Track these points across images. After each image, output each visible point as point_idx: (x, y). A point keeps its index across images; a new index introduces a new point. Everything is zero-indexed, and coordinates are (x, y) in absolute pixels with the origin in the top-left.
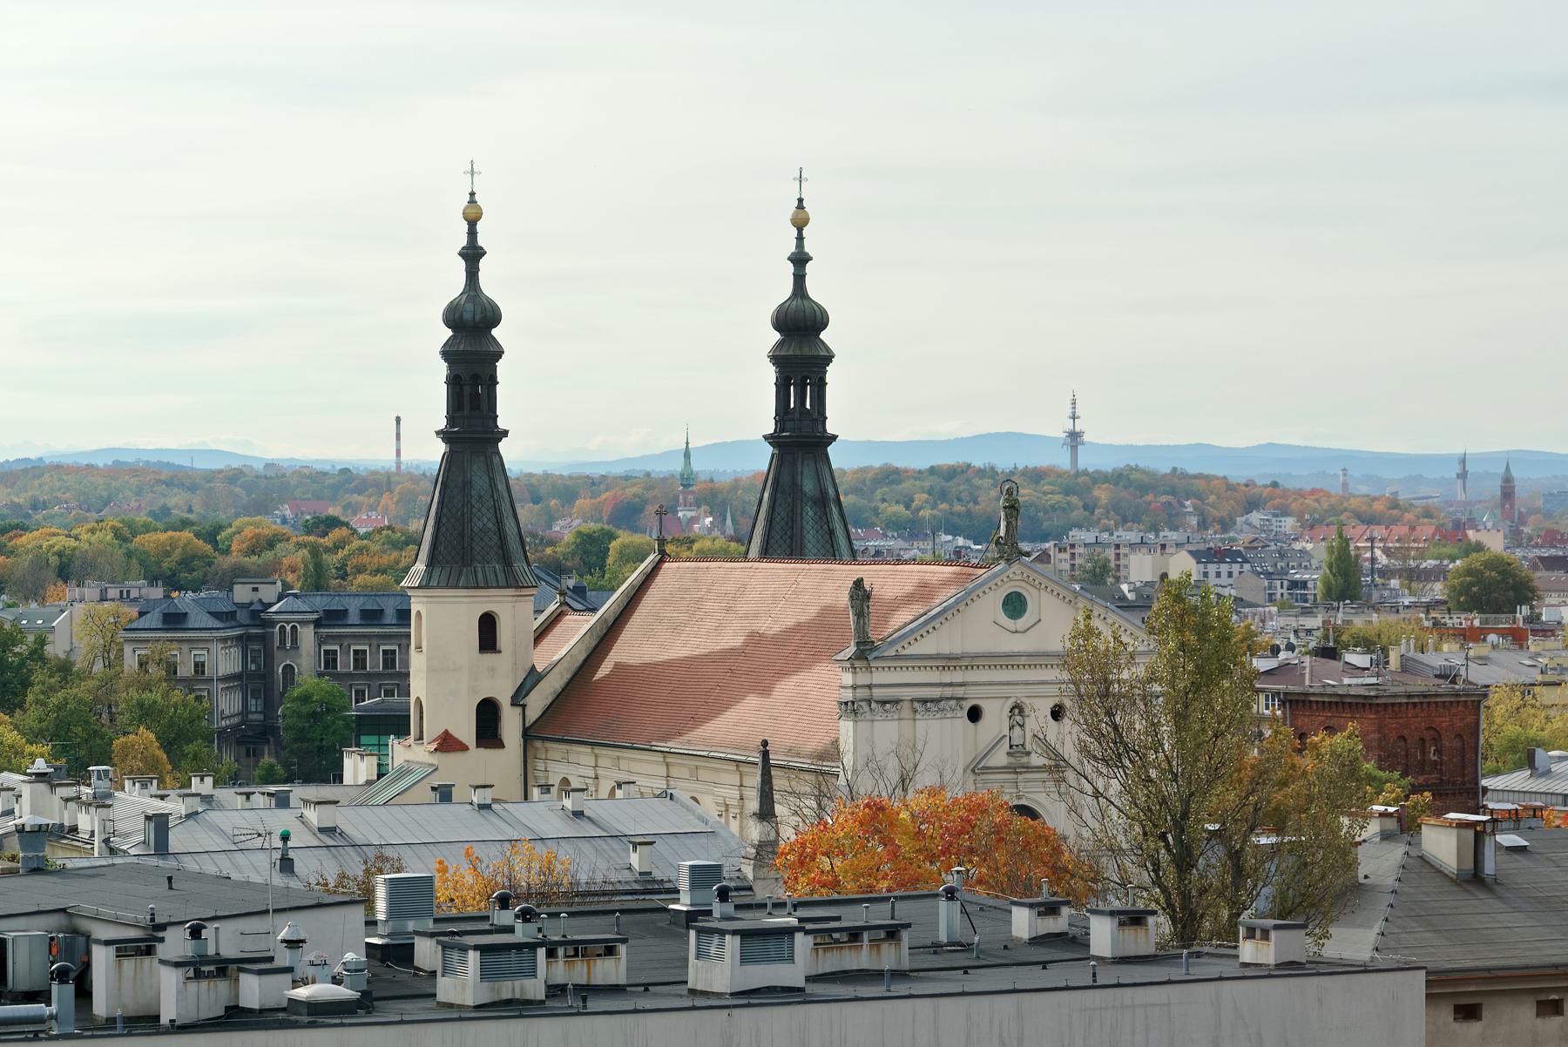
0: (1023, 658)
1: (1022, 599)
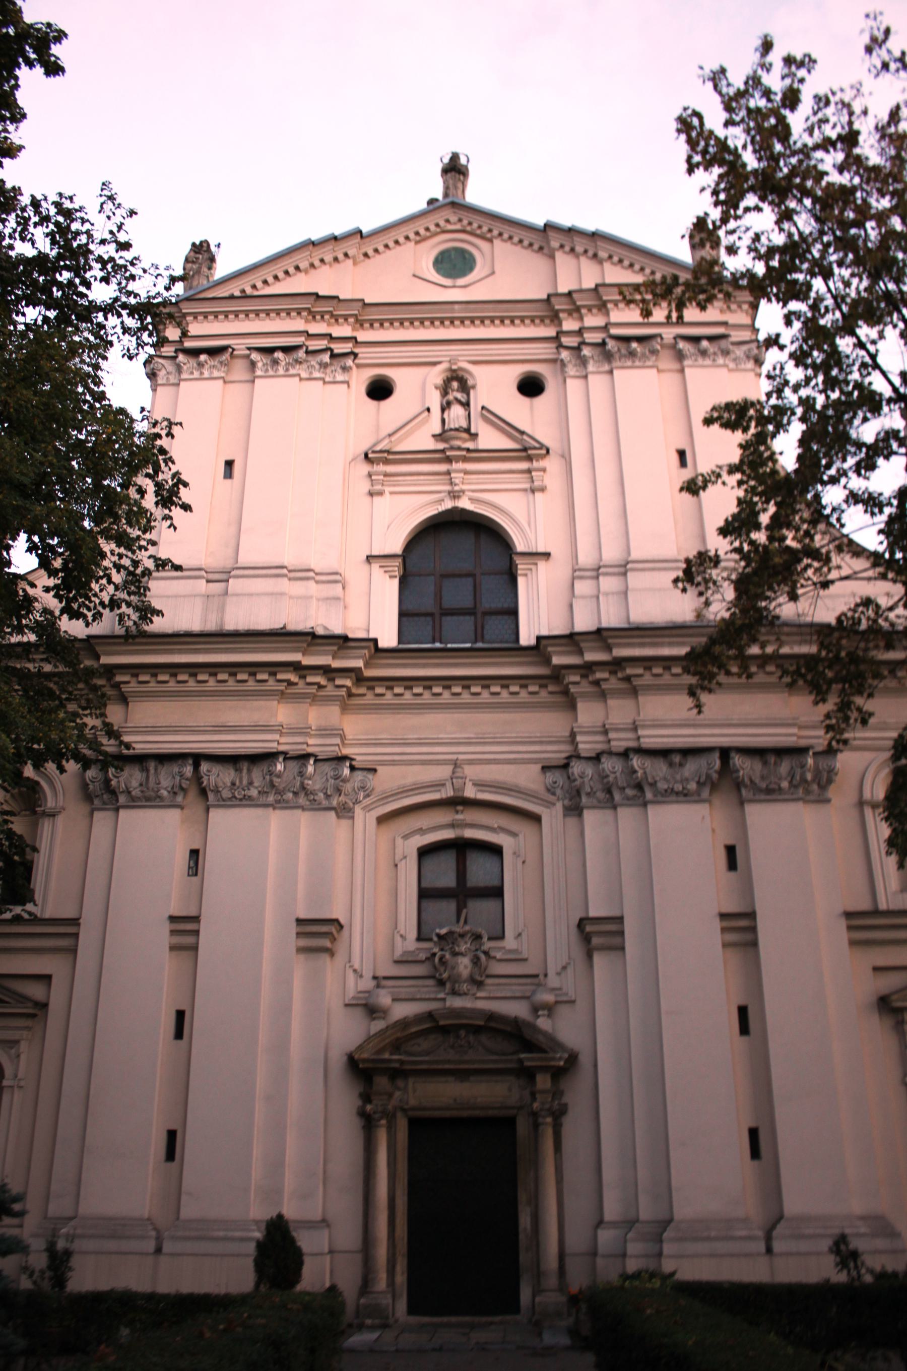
0: (456, 307)
1: (467, 256)
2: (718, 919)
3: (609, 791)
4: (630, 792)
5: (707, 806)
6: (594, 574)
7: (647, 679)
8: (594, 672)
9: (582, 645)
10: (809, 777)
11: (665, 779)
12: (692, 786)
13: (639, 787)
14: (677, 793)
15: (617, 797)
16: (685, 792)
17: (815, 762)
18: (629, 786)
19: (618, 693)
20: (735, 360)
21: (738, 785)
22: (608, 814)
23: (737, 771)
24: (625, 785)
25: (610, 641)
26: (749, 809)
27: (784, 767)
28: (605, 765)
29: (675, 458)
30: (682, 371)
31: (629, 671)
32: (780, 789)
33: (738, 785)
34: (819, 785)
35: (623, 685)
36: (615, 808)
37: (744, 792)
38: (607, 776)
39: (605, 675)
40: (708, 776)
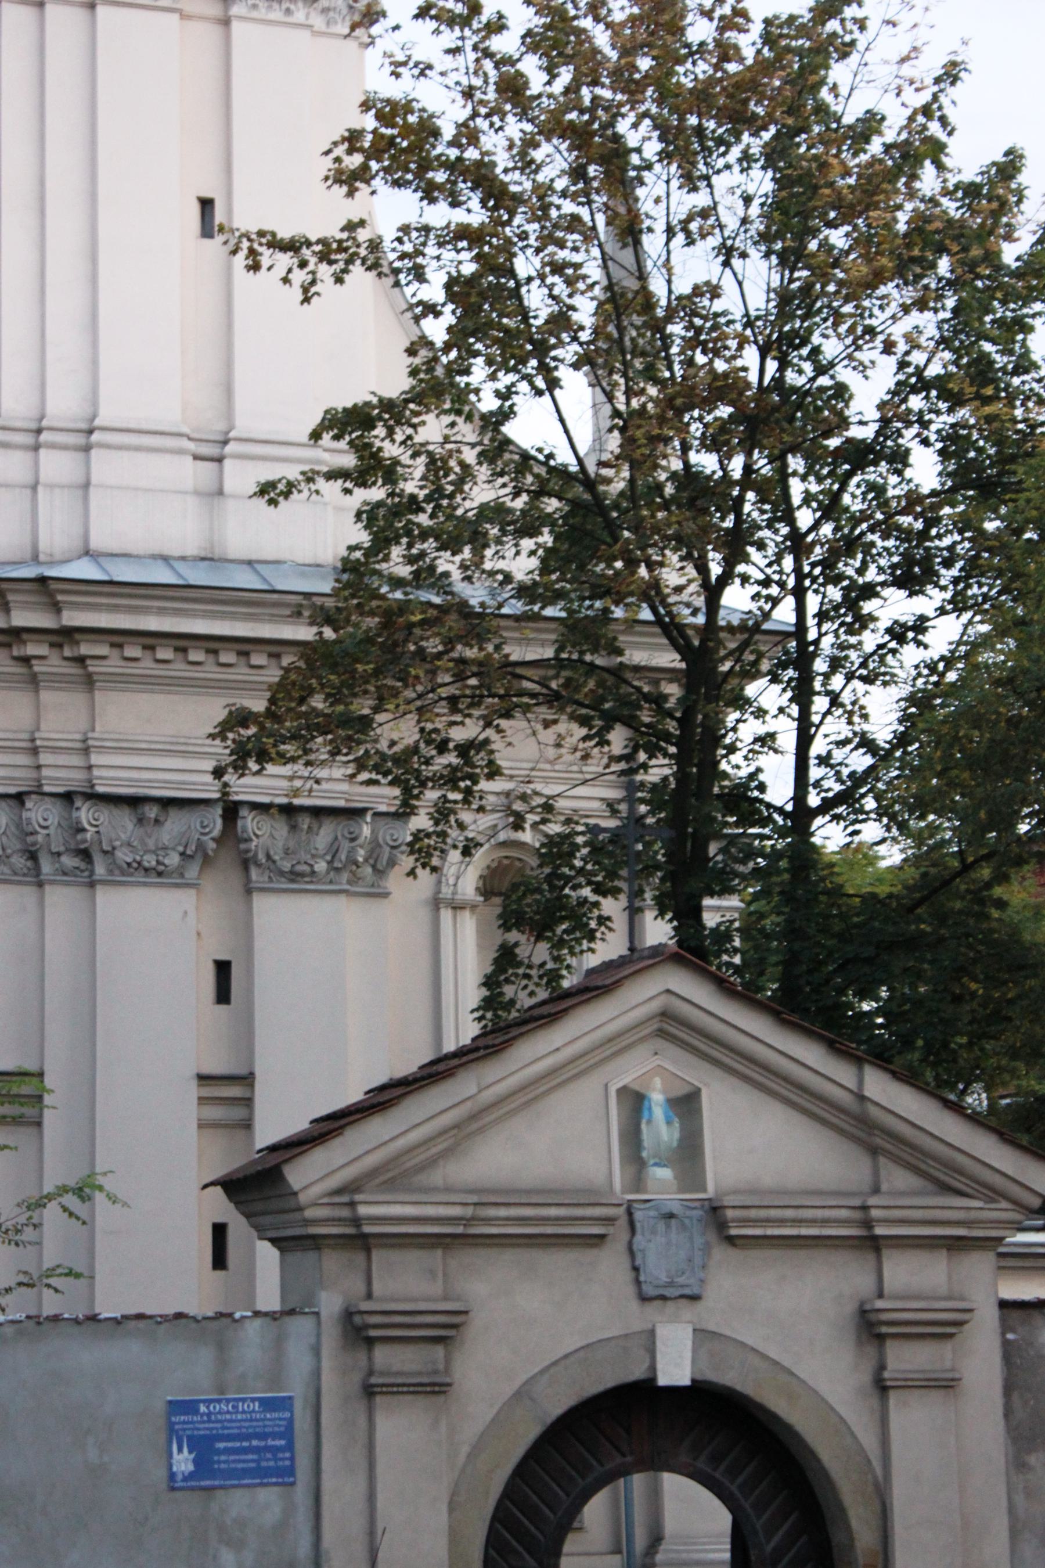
2: (194, 1083)
3: (33, 856)
4: (69, 861)
5: (192, 892)
6: (28, 439)
7: (114, 664)
8: (24, 643)
9: (10, 597)
10: (361, 855)
11: (129, 845)
12: (173, 860)
13: (85, 854)
14: (146, 870)
15: (47, 867)
16: (161, 868)
17: (373, 832)
18: (67, 850)
19: (58, 681)
20: (325, 10)
21: (246, 863)
22: (28, 893)
23: (248, 840)
24: (62, 849)
25: (60, 598)
26: (261, 903)
27: (325, 834)
28: (32, 815)
29: (195, 209)
30: (226, 22)
31: (84, 649)
32: (313, 872)
33: (246, 863)
34: (374, 867)
35: (74, 670)
36: (40, 885)
37: (254, 873)
38: (34, 833)
39: (42, 650)
40: (200, 845)
